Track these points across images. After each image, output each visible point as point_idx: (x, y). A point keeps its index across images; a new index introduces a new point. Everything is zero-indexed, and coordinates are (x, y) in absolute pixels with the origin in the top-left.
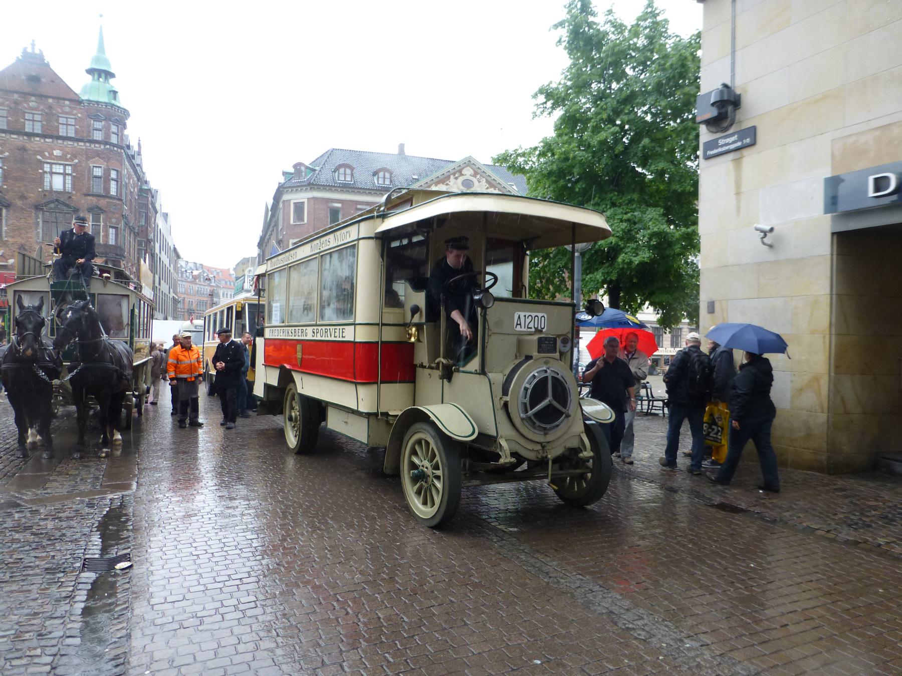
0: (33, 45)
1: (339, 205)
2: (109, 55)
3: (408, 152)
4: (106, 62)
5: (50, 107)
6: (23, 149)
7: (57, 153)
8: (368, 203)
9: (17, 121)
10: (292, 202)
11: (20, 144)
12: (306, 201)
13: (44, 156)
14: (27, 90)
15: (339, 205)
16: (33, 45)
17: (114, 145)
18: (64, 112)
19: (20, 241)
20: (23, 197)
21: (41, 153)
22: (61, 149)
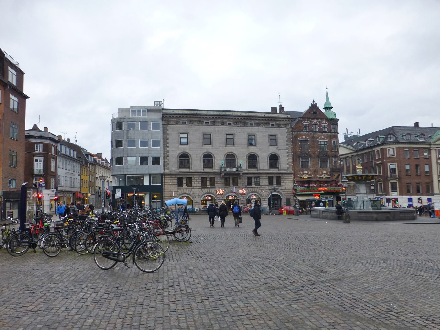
0: (314, 102)
1: (408, 149)
2: (330, 100)
3: (420, 125)
4: (330, 103)
5: (320, 122)
6: (313, 137)
7: (323, 137)
8: (418, 148)
9: (311, 128)
10: (387, 149)
11: (312, 135)
12: (395, 148)
13: (319, 139)
14: (313, 117)
15: (408, 149)
16: (314, 102)
17: (333, 133)
18: (324, 123)
19: (314, 169)
20: (314, 154)
21: (318, 138)
22: (324, 136)
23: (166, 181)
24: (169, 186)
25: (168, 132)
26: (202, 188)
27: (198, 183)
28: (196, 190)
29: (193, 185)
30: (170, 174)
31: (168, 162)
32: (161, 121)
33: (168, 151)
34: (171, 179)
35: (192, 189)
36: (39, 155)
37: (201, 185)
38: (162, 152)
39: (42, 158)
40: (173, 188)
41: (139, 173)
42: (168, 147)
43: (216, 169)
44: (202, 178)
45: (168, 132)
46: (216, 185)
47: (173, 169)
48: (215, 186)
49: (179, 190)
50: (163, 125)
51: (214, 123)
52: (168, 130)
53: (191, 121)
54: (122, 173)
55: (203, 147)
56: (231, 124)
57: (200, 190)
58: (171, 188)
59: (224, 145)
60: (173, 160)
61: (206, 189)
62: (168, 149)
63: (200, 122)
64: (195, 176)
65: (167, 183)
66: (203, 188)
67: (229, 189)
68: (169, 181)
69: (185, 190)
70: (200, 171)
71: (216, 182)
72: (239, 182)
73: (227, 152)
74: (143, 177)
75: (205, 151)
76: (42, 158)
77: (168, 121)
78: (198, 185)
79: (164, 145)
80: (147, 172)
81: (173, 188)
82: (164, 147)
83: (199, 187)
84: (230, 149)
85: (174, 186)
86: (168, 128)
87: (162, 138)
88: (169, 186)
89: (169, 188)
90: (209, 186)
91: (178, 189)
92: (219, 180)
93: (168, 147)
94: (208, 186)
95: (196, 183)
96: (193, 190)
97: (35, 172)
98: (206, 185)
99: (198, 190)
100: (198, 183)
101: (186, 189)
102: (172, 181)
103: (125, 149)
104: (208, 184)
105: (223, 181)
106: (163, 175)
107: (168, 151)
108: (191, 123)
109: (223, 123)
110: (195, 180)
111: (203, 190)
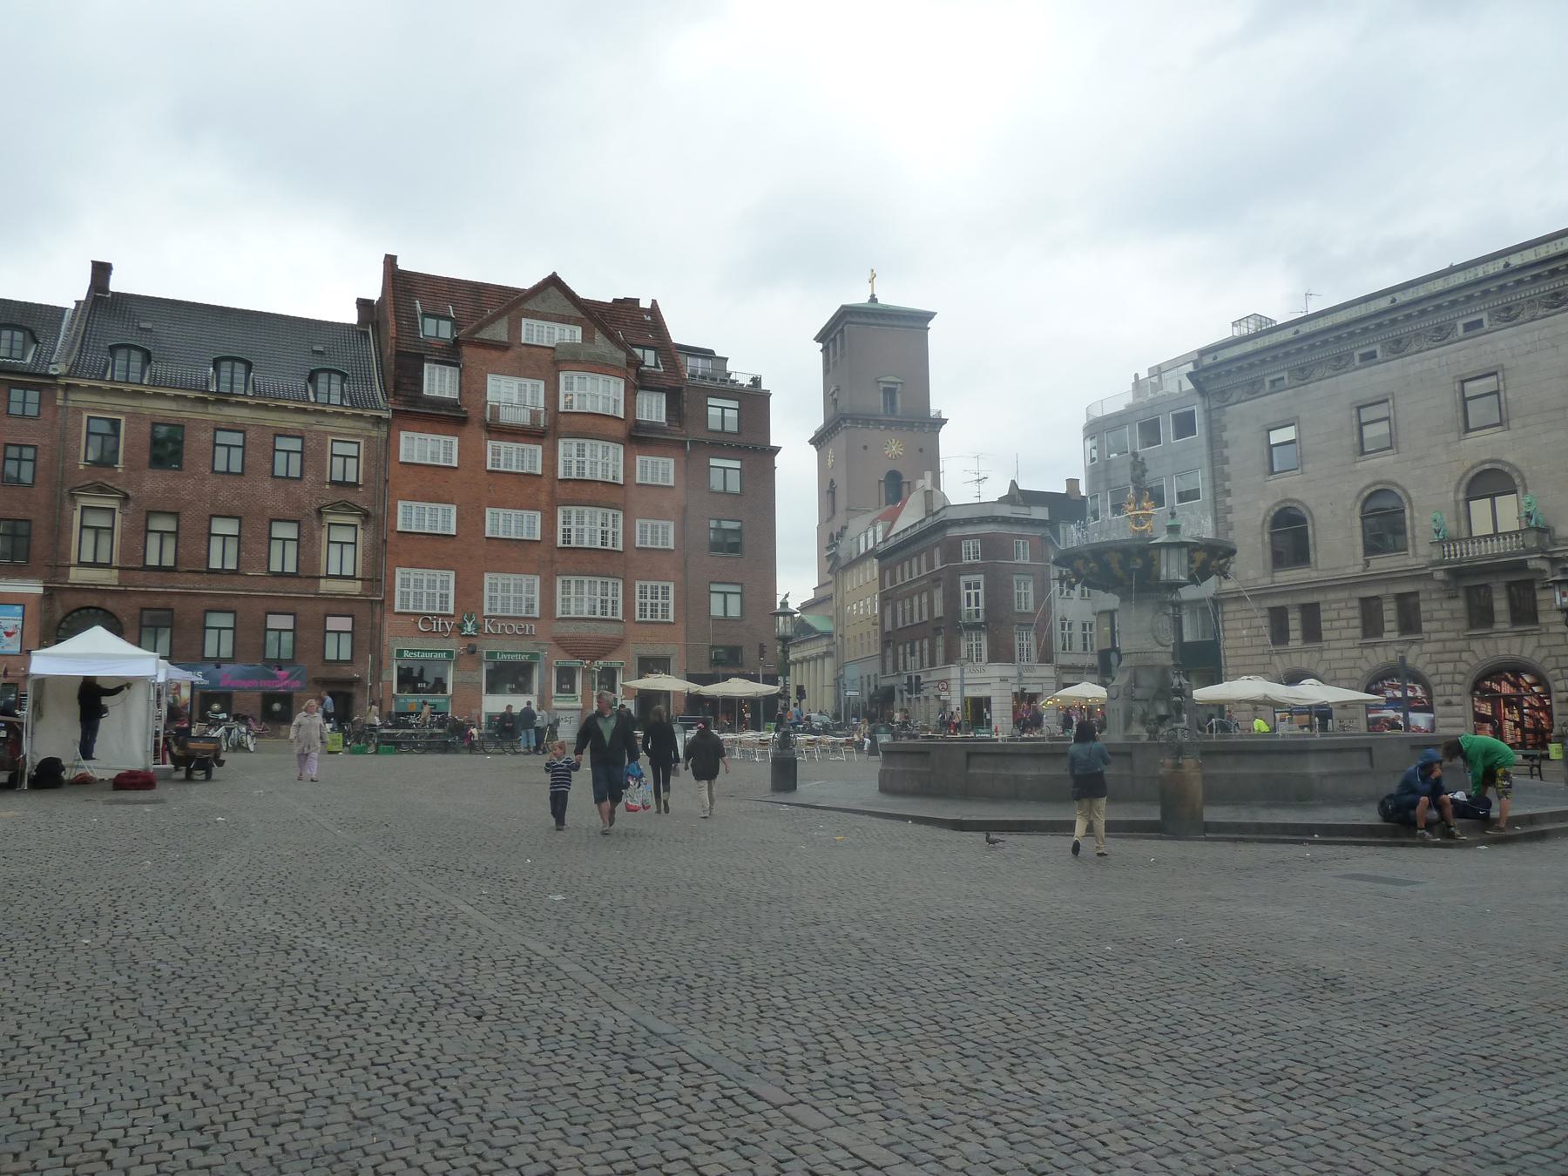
23: (1227, 625)
25: (1225, 436)
26: (1362, 646)
27: (1344, 623)
28: (1337, 654)
29: (1325, 635)
32: (1198, 399)
33: (1229, 510)
34: (1242, 615)
35: (1321, 650)
36: (972, 569)
37: (1358, 632)
39: (980, 578)
40: (1254, 651)
42: (1228, 493)
43: (1420, 551)
44: (1363, 600)
45: (1225, 436)
46: (1425, 626)
47: (1251, 574)
48: (1419, 631)
49: (1276, 659)
50: (1208, 412)
51: (1397, 348)
52: (1224, 428)
53: (1302, 370)
55: (1359, 466)
56: (1479, 323)
57: (1356, 653)
58: (1247, 651)
59: (1452, 437)
61: (1379, 650)
62: (1229, 501)
63: (1339, 359)
64: (1331, 596)
65: (1231, 634)
66: (1368, 645)
67: (1490, 644)
69: (1295, 656)
70: (1350, 572)
71: (1423, 616)
72: (1542, 607)
73: (1468, 465)
75: (1368, 480)
76: (980, 578)
77: (1223, 392)
78: (1345, 633)
81: (1254, 651)
82: (1215, 495)
83: (1350, 644)
84: (1483, 447)
87: (1205, 461)
89: (1240, 652)
90: (1395, 636)
91: (1270, 654)
92: (1436, 606)
93: (1228, 493)
94: (1387, 636)
95: (1336, 624)
96: (1327, 655)
97: (964, 619)
98: (1379, 632)
99: (1347, 654)
100: (1344, 623)
101: (1299, 651)
102: (1247, 623)
104: (1387, 626)
105: (1460, 605)
107: (1229, 510)
108: (1303, 374)
109: (1442, 335)
110: (1334, 615)
111: (1366, 652)
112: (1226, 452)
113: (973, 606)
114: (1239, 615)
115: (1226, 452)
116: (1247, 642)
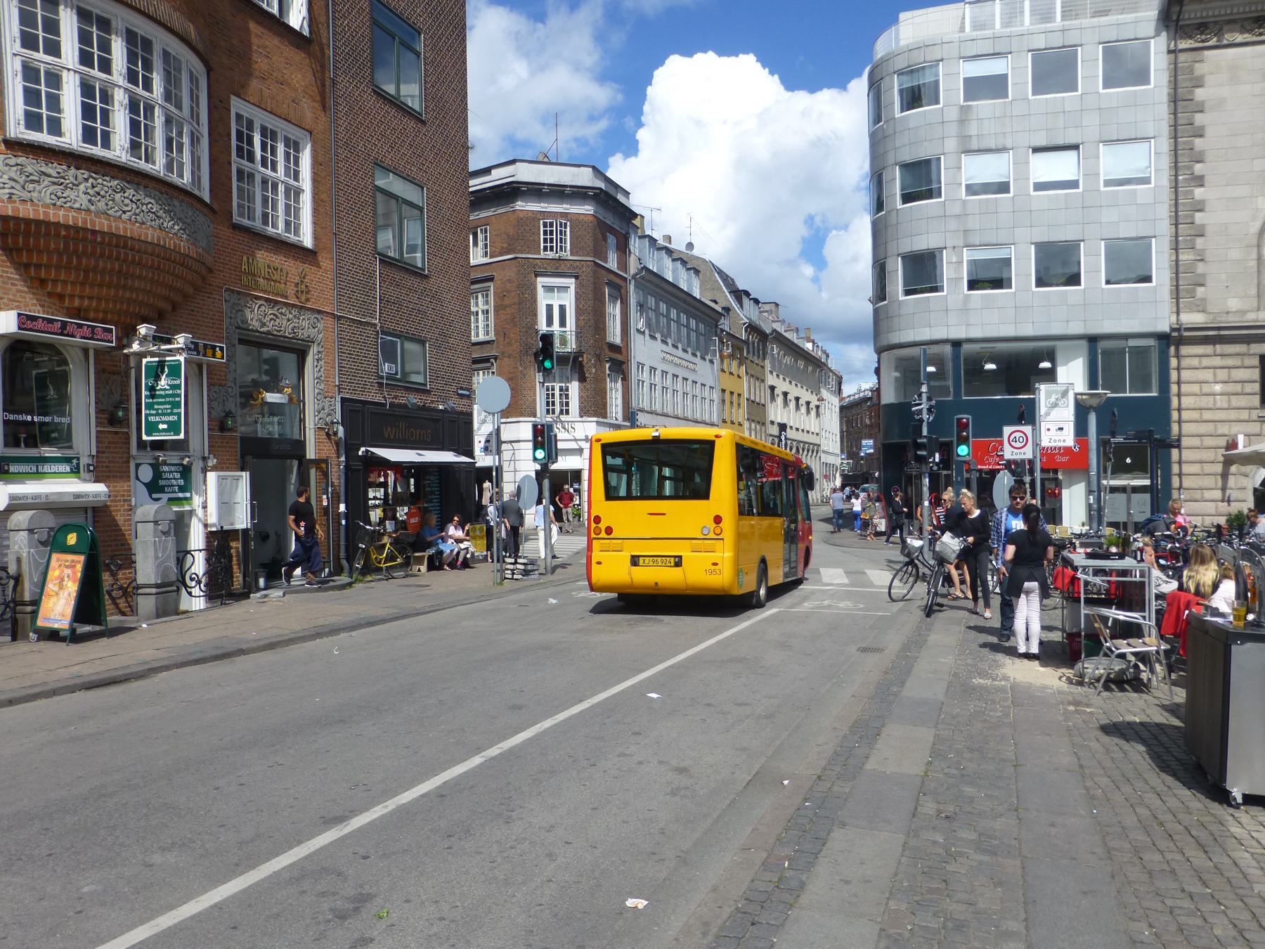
23: (1185, 375)
24: (1208, 402)
30: (1215, 337)
31: (1201, 268)
33: (1200, 207)
34: (1218, 361)
36: (557, 268)
38: (1164, 211)
40: (1233, 415)
41: (1028, 331)
45: (1200, 94)
47: (1234, 304)
52: (1199, 82)
54: (940, 334)
60: (1235, 254)
62: (1199, 193)
65: (1195, 388)
68: (1208, 375)
74: (1051, 356)
76: (571, 282)
79: (1176, 167)
80: (1076, 328)
81: (1233, 415)
85: (1235, 401)
86: (1200, 69)
88: (1208, 402)
89: (1207, 415)
93: (1200, 181)
102: (1222, 374)
103: (956, 209)
106: (1170, 340)
107: (1200, 207)
112: (1199, 119)
113: (556, 327)
114: (1206, 362)
115: (1199, 119)
116: (1221, 401)
